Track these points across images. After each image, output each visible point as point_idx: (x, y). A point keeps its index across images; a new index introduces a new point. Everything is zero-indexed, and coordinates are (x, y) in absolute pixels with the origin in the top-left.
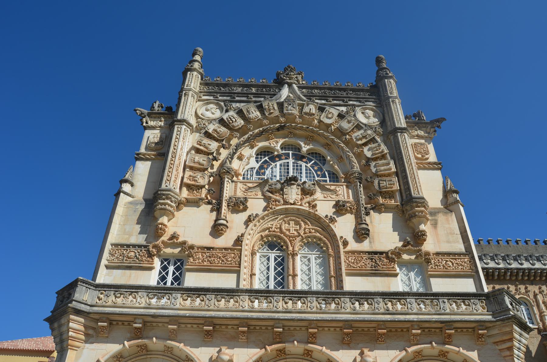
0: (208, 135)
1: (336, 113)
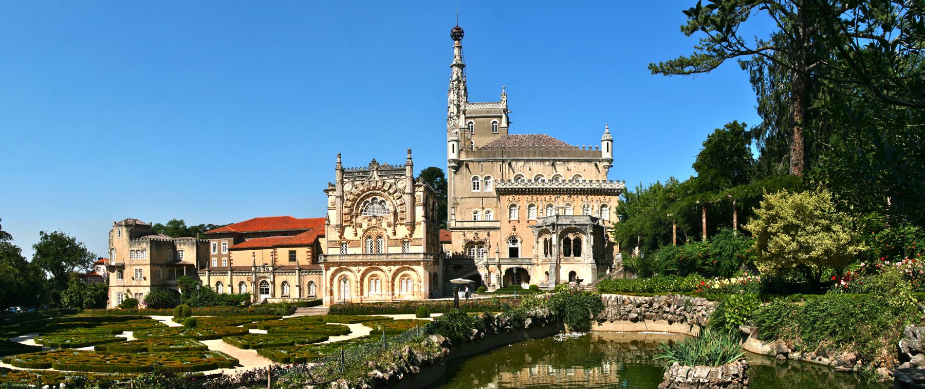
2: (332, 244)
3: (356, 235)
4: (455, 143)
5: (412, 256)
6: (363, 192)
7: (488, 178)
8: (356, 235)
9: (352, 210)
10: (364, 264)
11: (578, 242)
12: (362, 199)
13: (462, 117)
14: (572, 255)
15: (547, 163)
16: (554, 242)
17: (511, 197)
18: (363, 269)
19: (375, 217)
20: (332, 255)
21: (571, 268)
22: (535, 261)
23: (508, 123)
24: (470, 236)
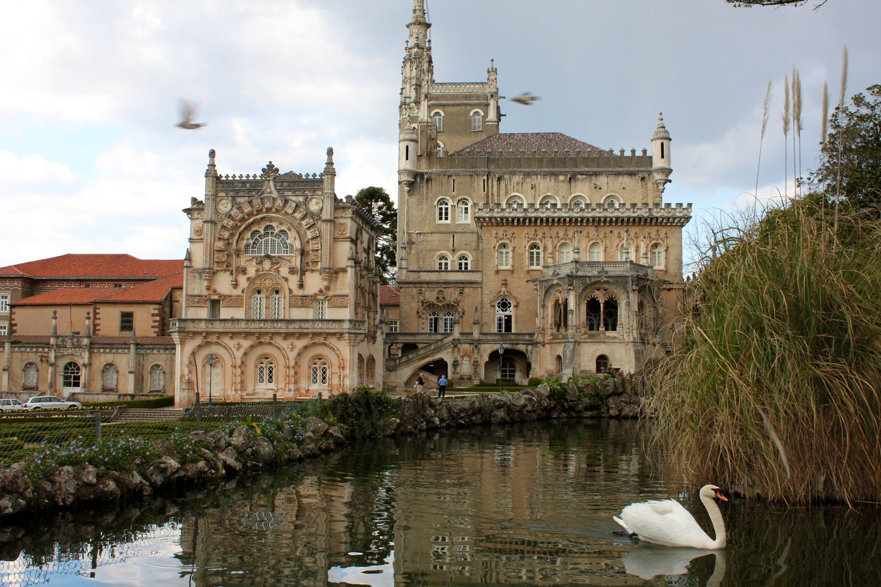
0: (223, 227)
1: (294, 205)
2: (196, 300)
3: (236, 286)
4: (411, 145)
5: (330, 325)
6: (250, 214)
7: (464, 201)
8: (236, 286)
9: (229, 244)
10: (247, 335)
11: (612, 306)
12: (248, 228)
13: (424, 104)
14: (602, 329)
15: (561, 178)
16: (572, 305)
17: (501, 230)
18: (246, 344)
19: (268, 257)
20: (193, 320)
21: (602, 349)
22: (540, 339)
23: (499, 116)
24: (431, 296)
